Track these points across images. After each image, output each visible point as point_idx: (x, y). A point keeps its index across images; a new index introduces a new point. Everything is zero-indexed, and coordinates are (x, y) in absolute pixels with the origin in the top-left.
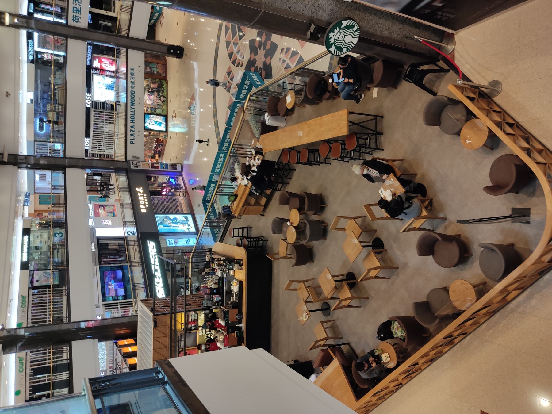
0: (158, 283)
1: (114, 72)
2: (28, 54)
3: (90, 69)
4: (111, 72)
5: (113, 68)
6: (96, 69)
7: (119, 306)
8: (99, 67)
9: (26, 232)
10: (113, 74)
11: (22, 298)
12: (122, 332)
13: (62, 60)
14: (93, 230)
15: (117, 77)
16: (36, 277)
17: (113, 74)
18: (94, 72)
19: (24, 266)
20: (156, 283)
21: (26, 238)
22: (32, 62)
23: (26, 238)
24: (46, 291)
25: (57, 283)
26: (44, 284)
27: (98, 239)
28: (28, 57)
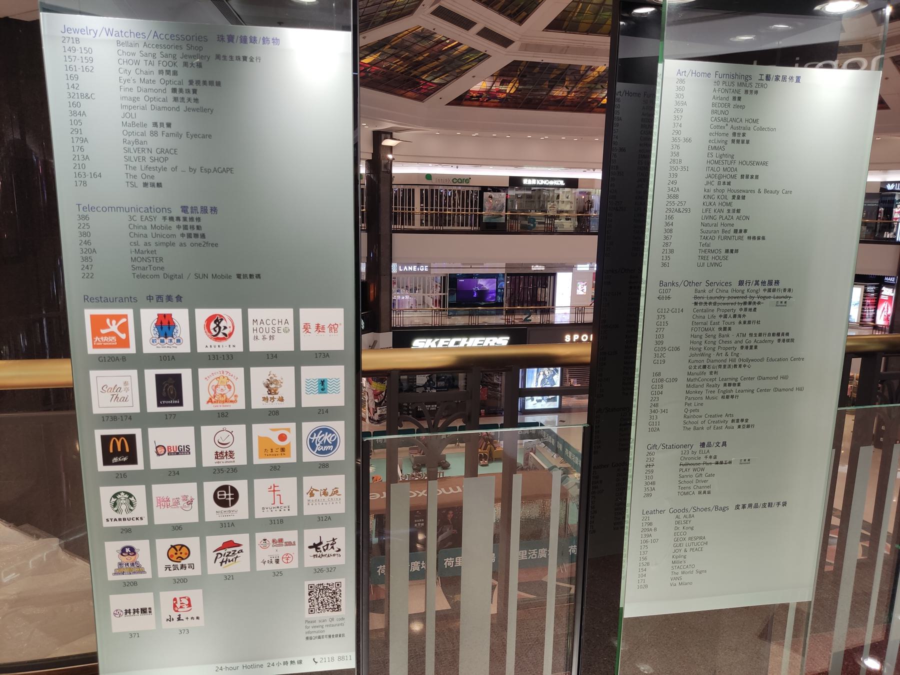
0: (437, 343)
1: (874, 321)
2: (895, 182)
3: (880, 281)
4: (874, 317)
5: (880, 321)
6: (878, 292)
7: (442, 294)
8: (882, 297)
9: (572, 183)
10: (868, 320)
11: (467, 179)
12: (372, 292)
13: (888, 235)
14: (569, 268)
15: (862, 323)
16: (495, 195)
17: (868, 320)
18: (871, 289)
19: (515, 182)
20: (437, 340)
21: (562, 183)
22: (883, 189)
23: (562, 183)
24: (476, 206)
25: (484, 219)
26: (486, 205)
27: (554, 275)
28: (891, 183)
